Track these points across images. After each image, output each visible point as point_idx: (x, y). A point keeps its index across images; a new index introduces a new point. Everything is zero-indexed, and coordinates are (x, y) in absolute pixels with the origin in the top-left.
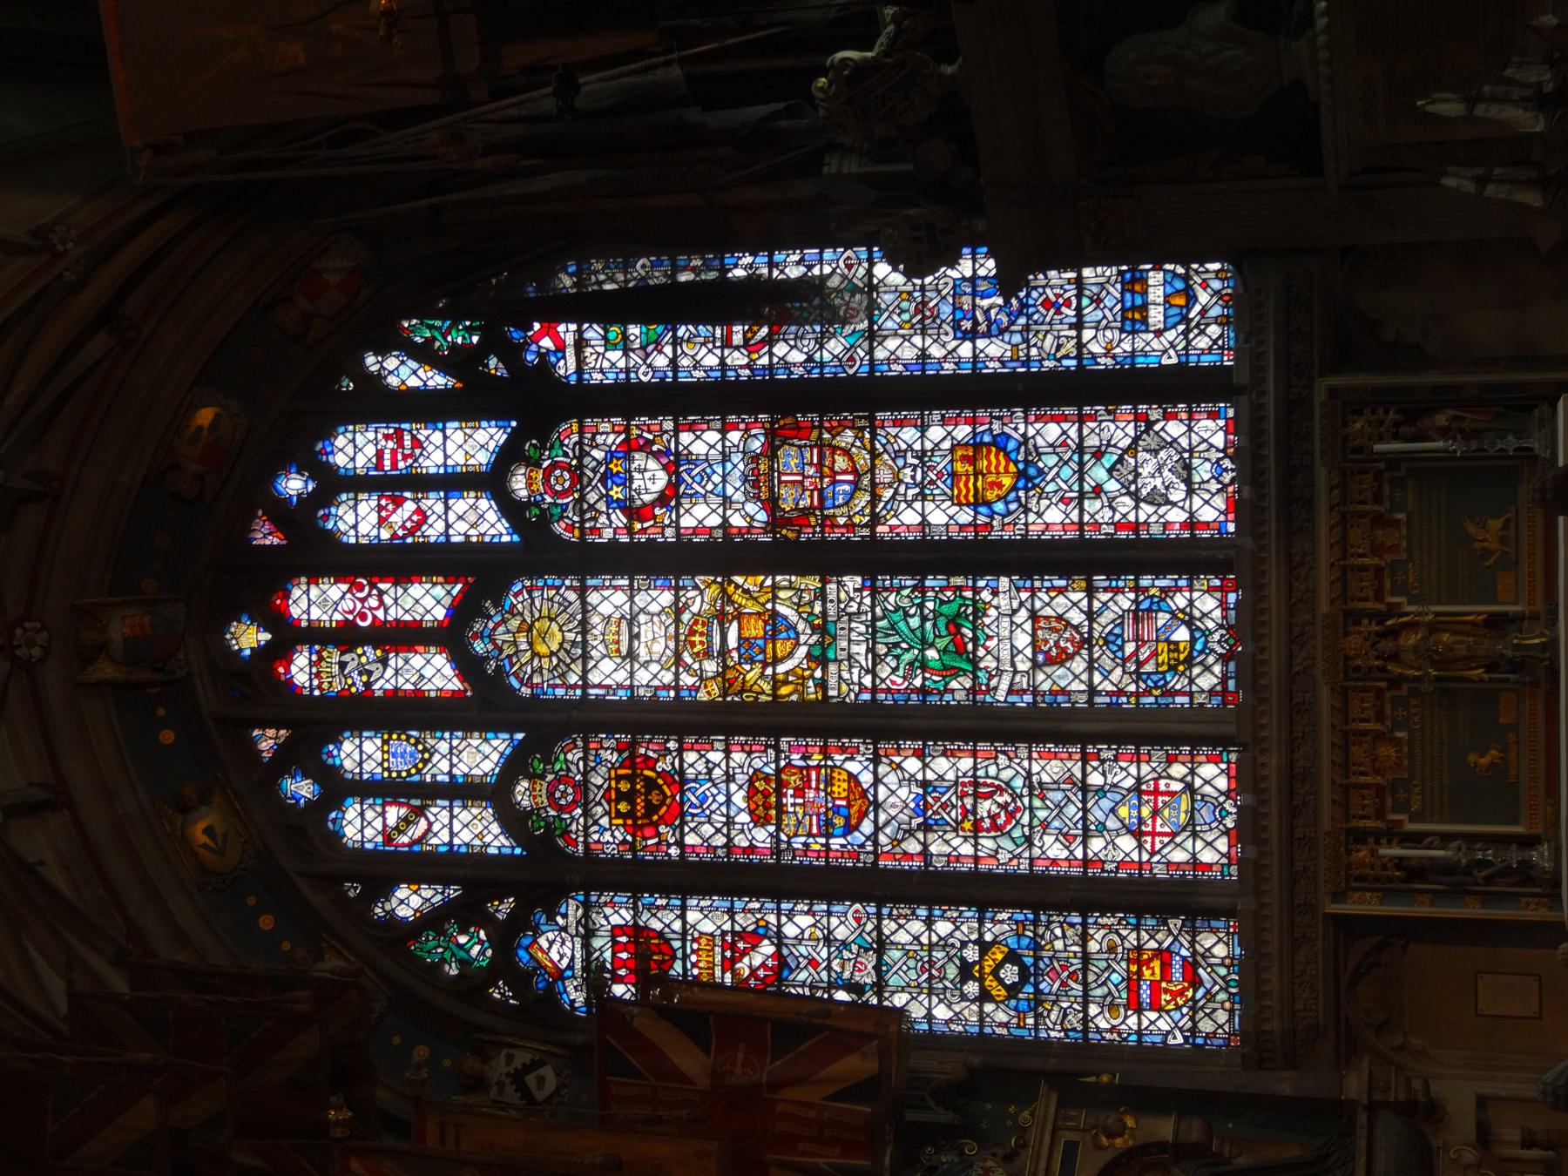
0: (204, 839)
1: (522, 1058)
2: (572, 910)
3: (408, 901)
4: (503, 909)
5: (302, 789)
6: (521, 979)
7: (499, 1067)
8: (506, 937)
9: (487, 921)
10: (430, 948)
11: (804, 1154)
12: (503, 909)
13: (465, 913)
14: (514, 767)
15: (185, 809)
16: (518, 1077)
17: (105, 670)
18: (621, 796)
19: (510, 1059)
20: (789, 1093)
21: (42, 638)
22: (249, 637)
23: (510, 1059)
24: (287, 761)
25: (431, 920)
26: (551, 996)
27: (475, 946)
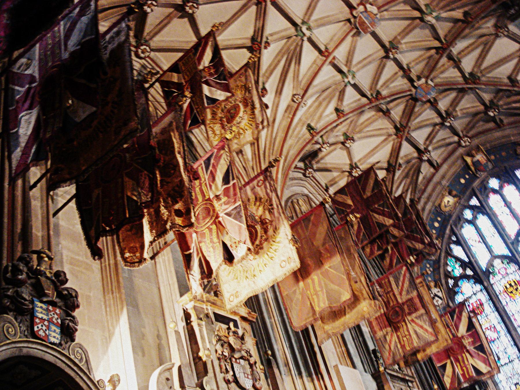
0: (446, 202)
1: (440, 294)
2: (478, 287)
3: (458, 251)
4: (469, 272)
5: (468, 214)
6: (456, 285)
7: (435, 291)
8: (464, 276)
9: (464, 270)
10: (451, 262)
11: (457, 366)
12: (469, 272)
13: (464, 265)
14: (503, 257)
15: (450, 193)
16: (436, 295)
17: (469, 160)
18: (510, 285)
19: (439, 292)
20: (468, 355)
21: (468, 144)
22: (494, 183)
23: (439, 292)
24: (472, 208)
25: (457, 259)
26: (456, 293)
27: (458, 271)
